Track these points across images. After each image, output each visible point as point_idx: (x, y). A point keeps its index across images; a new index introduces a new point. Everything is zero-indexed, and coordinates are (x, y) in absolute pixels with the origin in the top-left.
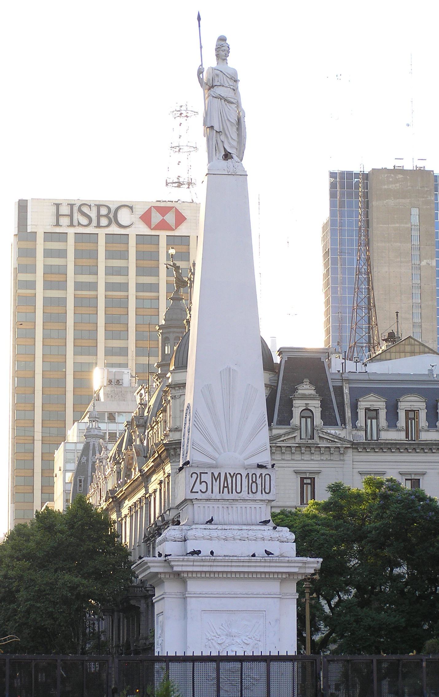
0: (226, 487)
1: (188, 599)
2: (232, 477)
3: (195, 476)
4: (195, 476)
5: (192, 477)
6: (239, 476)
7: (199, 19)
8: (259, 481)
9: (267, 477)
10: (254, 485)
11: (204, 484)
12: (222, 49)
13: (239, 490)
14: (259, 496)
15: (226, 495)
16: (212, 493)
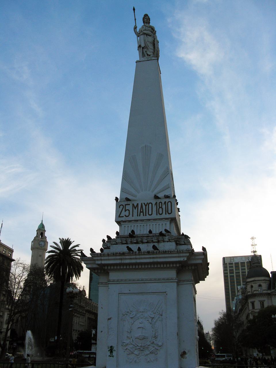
0: (142, 212)
1: (99, 287)
2: (146, 206)
3: (122, 207)
4: (122, 207)
5: (120, 207)
6: (150, 205)
7: (134, 9)
8: (164, 207)
9: (169, 203)
10: (161, 209)
11: (127, 211)
12: (146, 19)
13: (150, 213)
14: (164, 216)
15: (142, 217)
16: (133, 216)
